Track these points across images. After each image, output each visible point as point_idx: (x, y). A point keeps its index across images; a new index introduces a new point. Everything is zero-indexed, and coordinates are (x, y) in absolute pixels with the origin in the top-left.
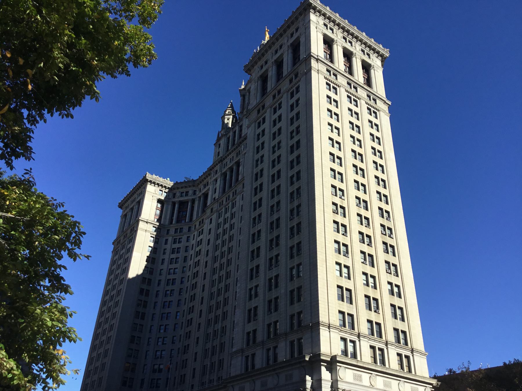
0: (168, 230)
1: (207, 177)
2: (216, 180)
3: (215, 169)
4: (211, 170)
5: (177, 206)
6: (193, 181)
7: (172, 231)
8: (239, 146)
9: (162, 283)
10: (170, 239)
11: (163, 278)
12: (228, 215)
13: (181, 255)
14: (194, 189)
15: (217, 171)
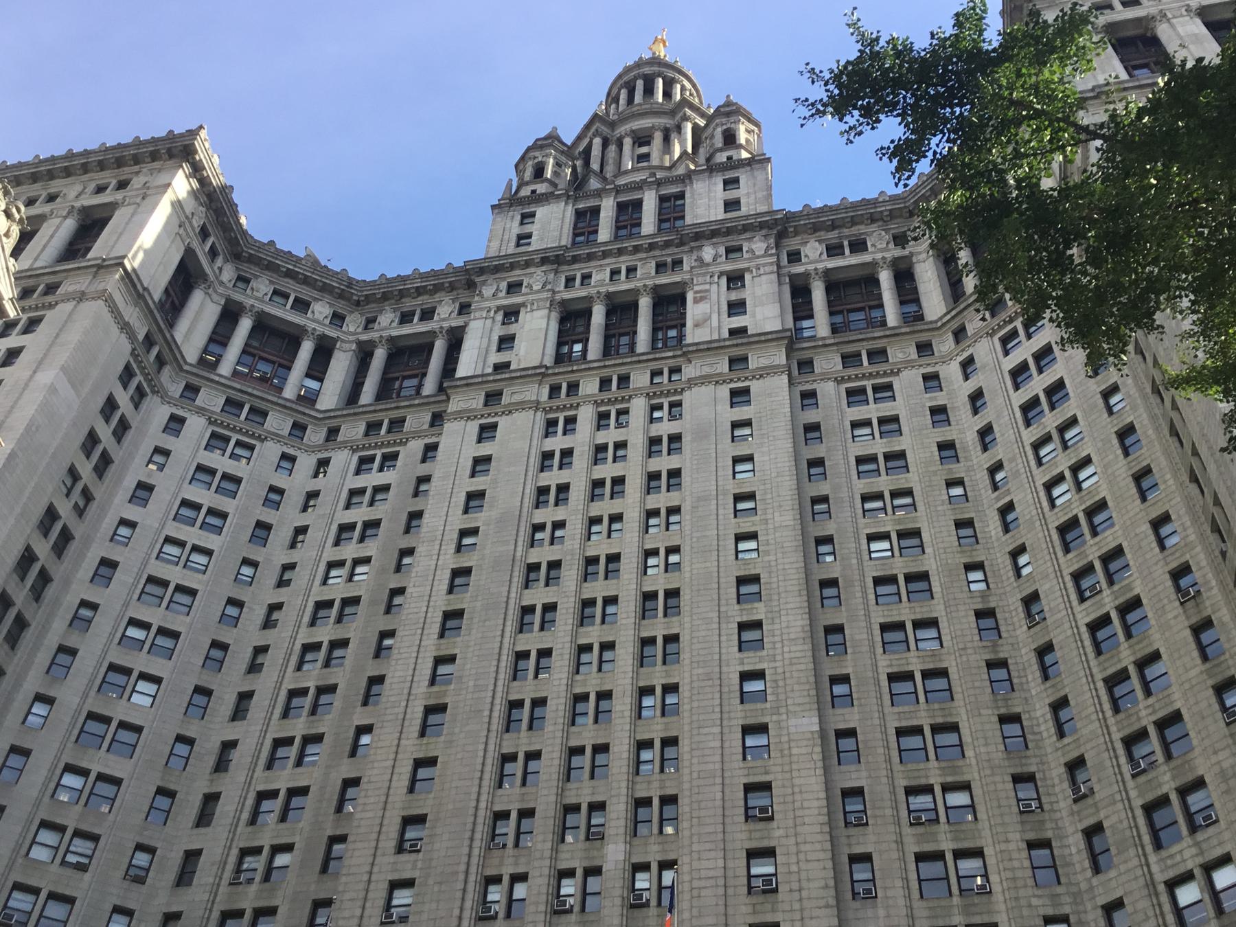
0: (191, 390)
1: (437, 288)
2: (511, 314)
3: (514, 275)
4: (482, 271)
5: (245, 325)
6: (351, 282)
7: (211, 399)
8: (682, 244)
9: (122, 577)
10: (196, 427)
11: (134, 561)
12: (636, 431)
13: (243, 508)
14: (341, 307)
15: (514, 287)
